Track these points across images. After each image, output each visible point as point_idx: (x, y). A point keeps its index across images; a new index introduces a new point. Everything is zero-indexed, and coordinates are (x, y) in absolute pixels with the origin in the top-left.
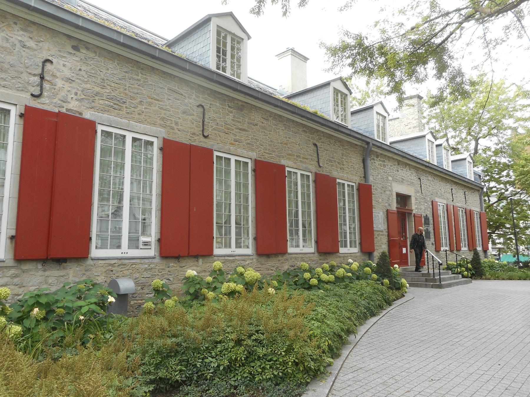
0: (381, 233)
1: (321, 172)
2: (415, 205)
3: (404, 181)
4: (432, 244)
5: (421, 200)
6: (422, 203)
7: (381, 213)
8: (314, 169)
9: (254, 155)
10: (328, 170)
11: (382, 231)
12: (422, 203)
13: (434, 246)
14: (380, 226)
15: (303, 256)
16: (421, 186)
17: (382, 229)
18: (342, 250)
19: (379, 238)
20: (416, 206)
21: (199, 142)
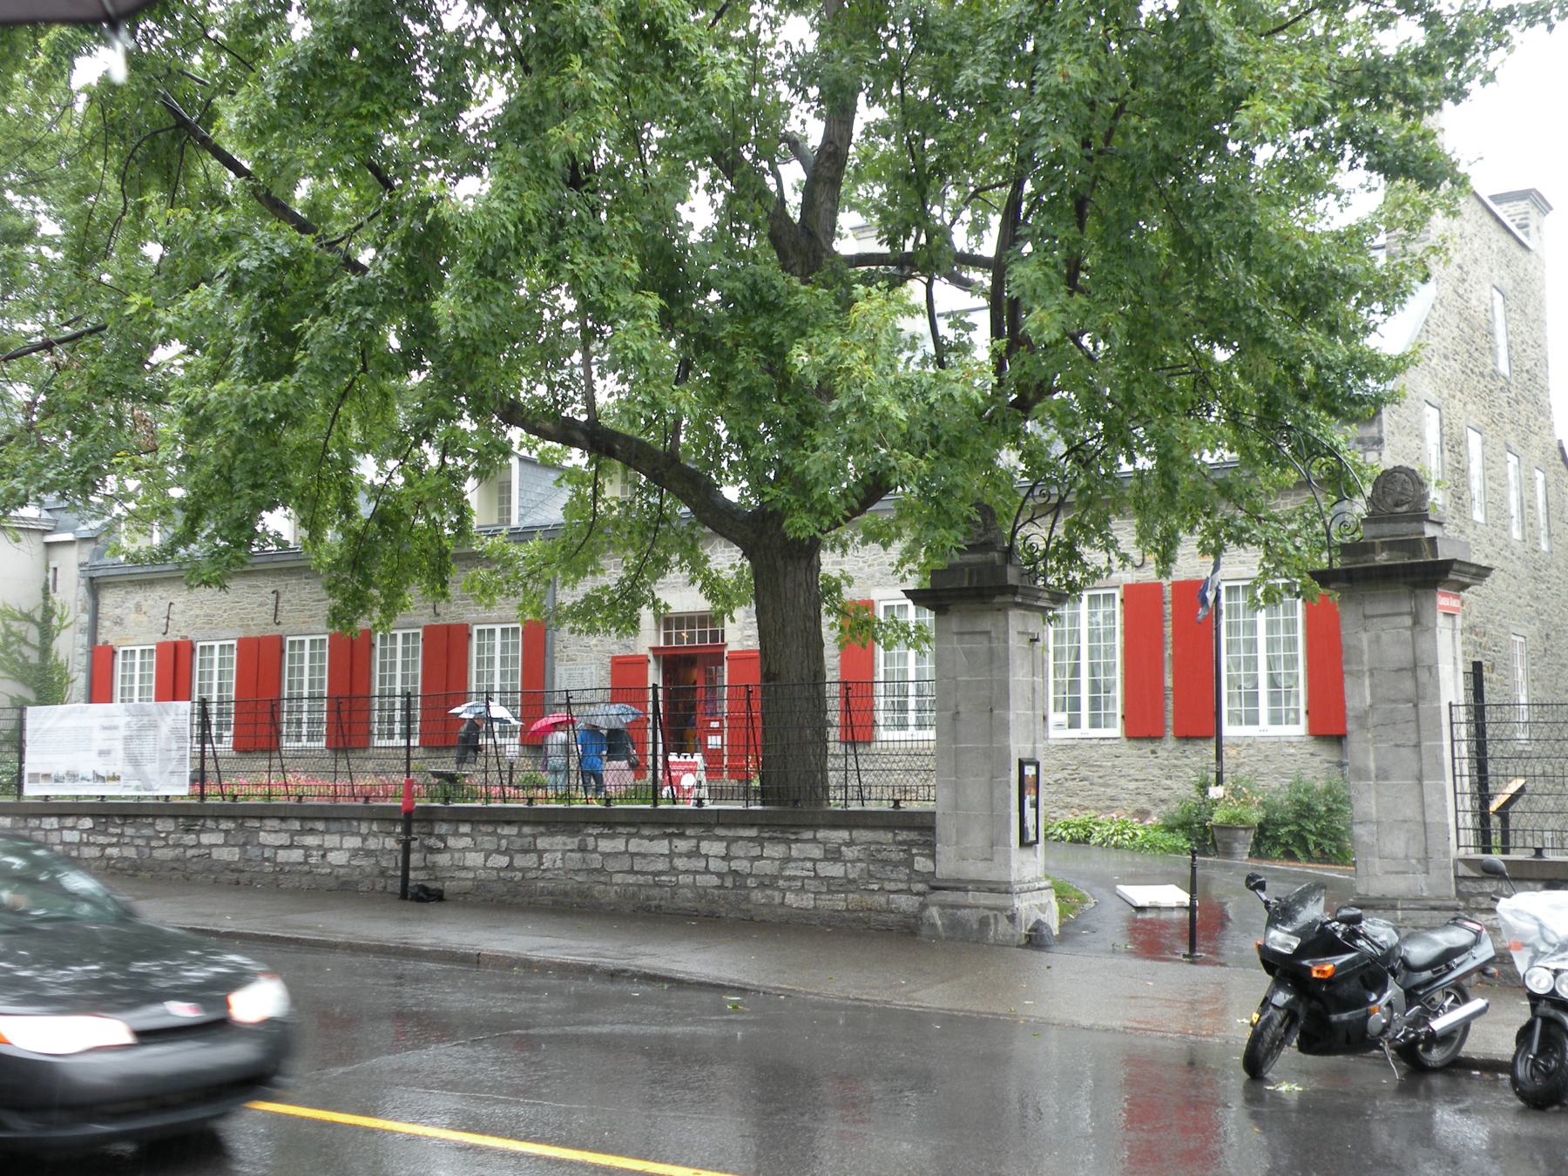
1: (441, 622)
10: (451, 613)
21: (274, 631)
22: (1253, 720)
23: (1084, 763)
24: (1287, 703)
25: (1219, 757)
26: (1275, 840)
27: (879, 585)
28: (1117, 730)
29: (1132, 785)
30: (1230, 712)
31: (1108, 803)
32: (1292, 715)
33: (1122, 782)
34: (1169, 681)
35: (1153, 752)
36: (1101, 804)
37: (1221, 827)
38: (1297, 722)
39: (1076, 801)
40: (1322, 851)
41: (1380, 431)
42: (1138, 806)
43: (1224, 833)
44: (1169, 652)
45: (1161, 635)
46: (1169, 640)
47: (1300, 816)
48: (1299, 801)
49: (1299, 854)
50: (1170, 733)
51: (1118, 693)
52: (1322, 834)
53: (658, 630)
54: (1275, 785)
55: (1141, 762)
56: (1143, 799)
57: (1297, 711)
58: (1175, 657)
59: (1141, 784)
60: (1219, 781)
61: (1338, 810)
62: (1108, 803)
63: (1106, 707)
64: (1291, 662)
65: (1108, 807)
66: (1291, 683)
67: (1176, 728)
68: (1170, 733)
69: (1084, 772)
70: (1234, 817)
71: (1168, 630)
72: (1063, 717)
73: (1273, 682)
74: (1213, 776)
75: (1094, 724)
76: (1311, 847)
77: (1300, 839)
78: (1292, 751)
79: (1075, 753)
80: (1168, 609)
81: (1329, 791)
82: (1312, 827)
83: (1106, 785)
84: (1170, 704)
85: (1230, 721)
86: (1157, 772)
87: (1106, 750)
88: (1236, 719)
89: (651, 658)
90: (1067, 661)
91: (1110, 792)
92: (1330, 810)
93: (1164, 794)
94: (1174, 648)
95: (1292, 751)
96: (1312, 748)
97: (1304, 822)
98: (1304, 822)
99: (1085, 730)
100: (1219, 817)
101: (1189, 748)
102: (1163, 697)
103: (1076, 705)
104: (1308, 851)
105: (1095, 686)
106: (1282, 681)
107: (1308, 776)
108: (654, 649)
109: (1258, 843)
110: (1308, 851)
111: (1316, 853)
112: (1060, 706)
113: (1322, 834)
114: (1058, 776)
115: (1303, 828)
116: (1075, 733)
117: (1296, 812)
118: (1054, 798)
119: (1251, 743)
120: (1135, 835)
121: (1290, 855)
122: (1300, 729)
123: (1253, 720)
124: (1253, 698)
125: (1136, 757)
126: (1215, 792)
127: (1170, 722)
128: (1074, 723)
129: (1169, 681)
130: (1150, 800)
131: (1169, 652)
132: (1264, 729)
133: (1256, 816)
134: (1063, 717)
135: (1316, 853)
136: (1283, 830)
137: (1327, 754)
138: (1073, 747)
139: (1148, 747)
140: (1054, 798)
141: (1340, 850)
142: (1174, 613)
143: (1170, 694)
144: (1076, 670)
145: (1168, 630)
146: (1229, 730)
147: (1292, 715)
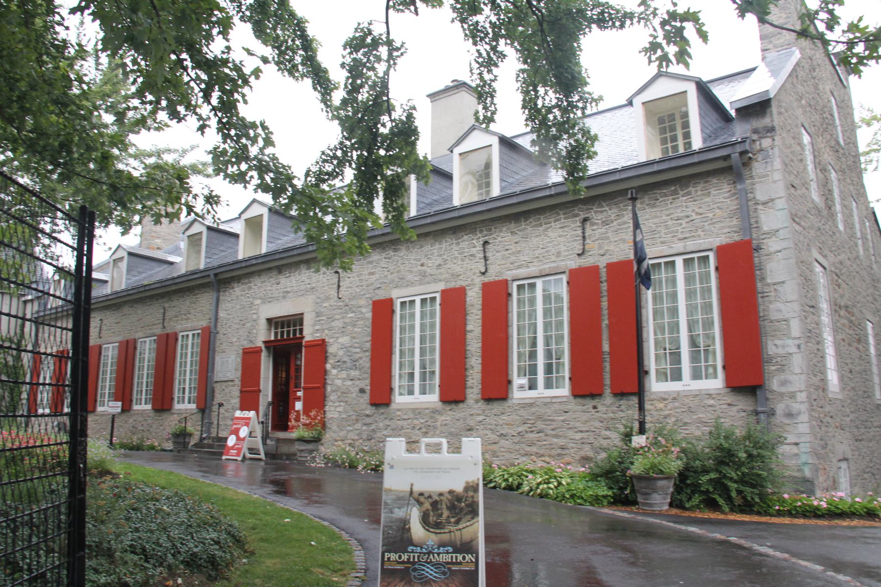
0: (230, 383)
2: (315, 325)
3: (290, 294)
4: (362, 391)
5: (335, 312)
6: (337, 317)
7: (233, 357)
8: (158, 331)
9: (120, 338)
11: (232, 381)
12: (337, 317)
13: (367, 397)
14: (229, 374)
15: (142, 413)
16: (339, 286)
17: (231, 378)
18: (136, 407)
19: (227, 390)
20: (317, 327)
22: (677, 376)
23: (540, 418)
24: (706, 361)
25: (641, 408)
26: (696, 488)
27: (397, 287)
28: (564, 391)
29: (578, 436)
30: (657, 371)
31: (559, 451)
32: (711, 370)
33: (570, 434)
34: (606, 347)
35: (595, 407)
36: (554, 452)
37: (640, 478)
38: (716, 377)
39: (534, 449)
40: (744, 498)
41: (772, 121)
42: (582, 453)
43: (644, 484)
44: (605, 322)
45: (599, 308)
46: (605, 312)
47: (721, 462)
48: (720, 448)
49: (721, 501)
50: (608, 391)
51: (566, 359)
52: (742, 481)
53: (270, 330)
54: (698, 433)
55: (585, 416)
56: (587, 448)
57: (715, 367)
58: (610, 326)
59: (584, 435)
60: (642, 431)
61: (759, 455)
62: (559, 451)
63: (557, 372)
64: (708, 324)
65: (559, 455)
66: (710, 343)
67: (612, 386)
68: (608, 391)
69: (540, 425)
70: (653, 467)
71: (605, 304)
72: (524, 381)
73: (693, 343)
74: (636, 426)
75: (548, 385)
76: (734, 494)
77: (720, 485)
78: (712, 402)
79: (533, 410)
80: (604, 287)
81: (748, 437)
82: (733, 475)
83: (557, 436)
84: (607, 366)
85: (658, 380)
86: (597, 424)
87: (557, 406)
88: (662, 376)
89: (263, 348)
90: (527, 335)
91: (561, 442)
92: (750, 456)
93: (605, 443)
94: (609, 319)
95: (712, 402)
96: (731, 398)
97: (726, 470)
98: (726, 470)
99: (541, 391)
100: (637, 468)
101: (624, 402)
102: (601, 361)
103: (533, 370)
104: (729, 499)
105: (548, 354)
106: (701, 342)
107: (726, 423)
108: (265, 342)
109: (678, 489)
110: (729, 499)
111: (738, 501)
112: (521, 372)
113: (742, 481)
114: (520, 429)
115: (725, 476)
116: (533, 394)
117: (716, 458)
118: (517, 447)
119: (676, 397)
120: (560, 484)
121: (712, 505)
122: (717, 383)
123: (677, 376)
124: (676, 357)
125: (581, 410)
126: (639, 441)
127: (607, 381)
128: (532, 386)
129: (606, 347)
130: (592, 448)
131: (605, 322)
132: (687, 384)
133: (674, 465)
134: (524, 381)
135: (738, 501)
136: (705, 478)
137: (743, 403)
138: (531, 405)
139: (590, 403)
140: (517, 447)
141: (762, 496)
142: (608, 291)
143: (607, 358)
144: (534, 344)
145: (605, 304)
146: (655, 386)
147: (711, 370)
